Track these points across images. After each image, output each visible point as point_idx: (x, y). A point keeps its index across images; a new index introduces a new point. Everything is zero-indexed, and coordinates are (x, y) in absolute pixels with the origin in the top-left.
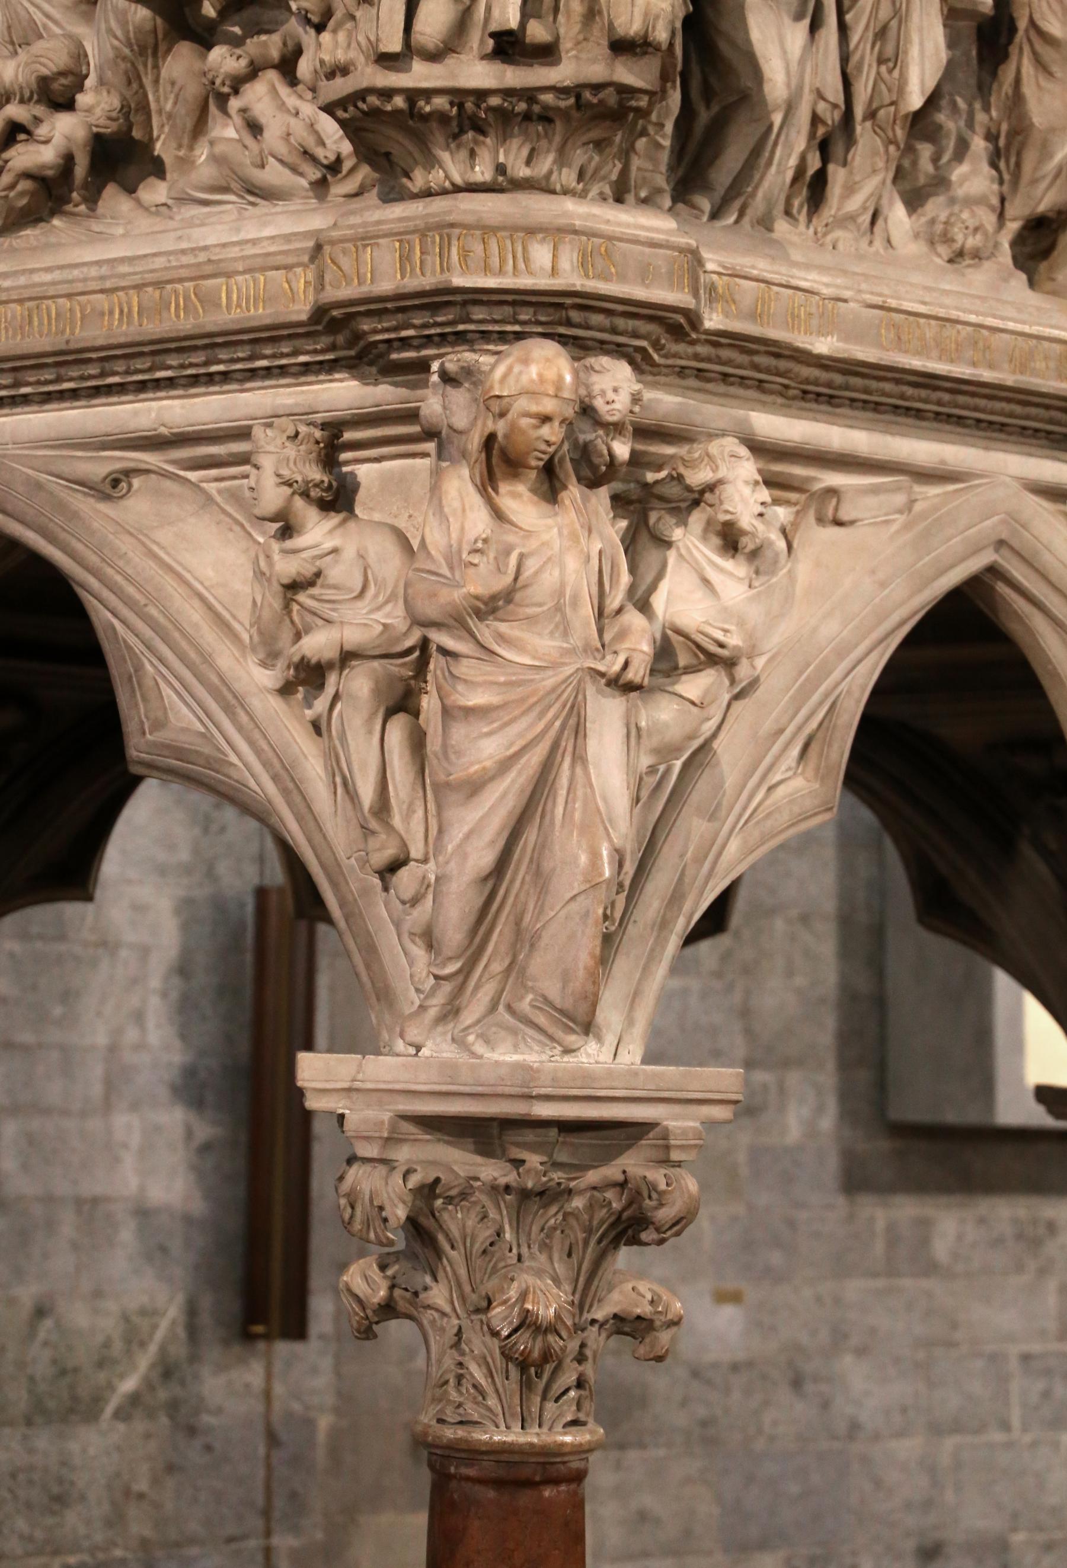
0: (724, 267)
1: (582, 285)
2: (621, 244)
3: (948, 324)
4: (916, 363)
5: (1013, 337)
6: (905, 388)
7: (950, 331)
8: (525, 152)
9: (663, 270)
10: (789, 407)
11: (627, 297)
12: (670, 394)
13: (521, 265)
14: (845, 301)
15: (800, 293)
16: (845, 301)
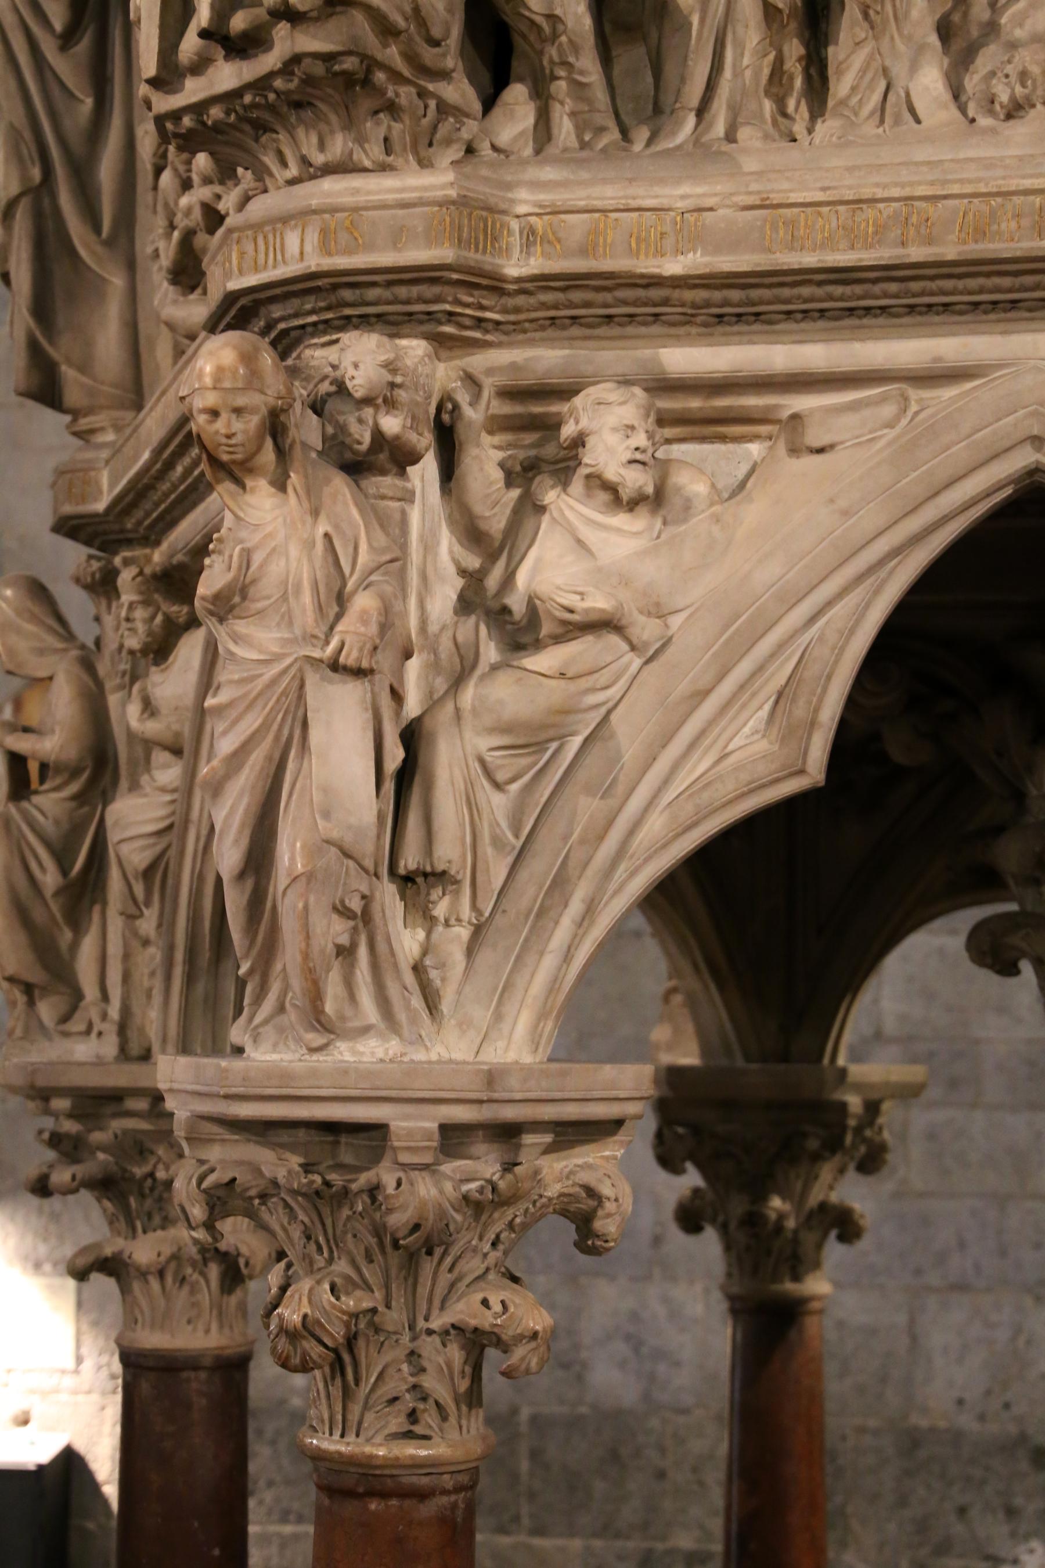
0: (541, 206)
1: (318, 265)
2: (370, 213)
3: (864, 206)
4: (810, 260)
5: (966, 201)
6: (830, 289)
7: (870, 213)
8: (314, 139)
9: (420, 229)
10: (711, 335)
11: (370, 266)
12: (553, 348)
13: (279, 257)
14: (711, 209)
15: (649, 213)
16: (711, 209)
